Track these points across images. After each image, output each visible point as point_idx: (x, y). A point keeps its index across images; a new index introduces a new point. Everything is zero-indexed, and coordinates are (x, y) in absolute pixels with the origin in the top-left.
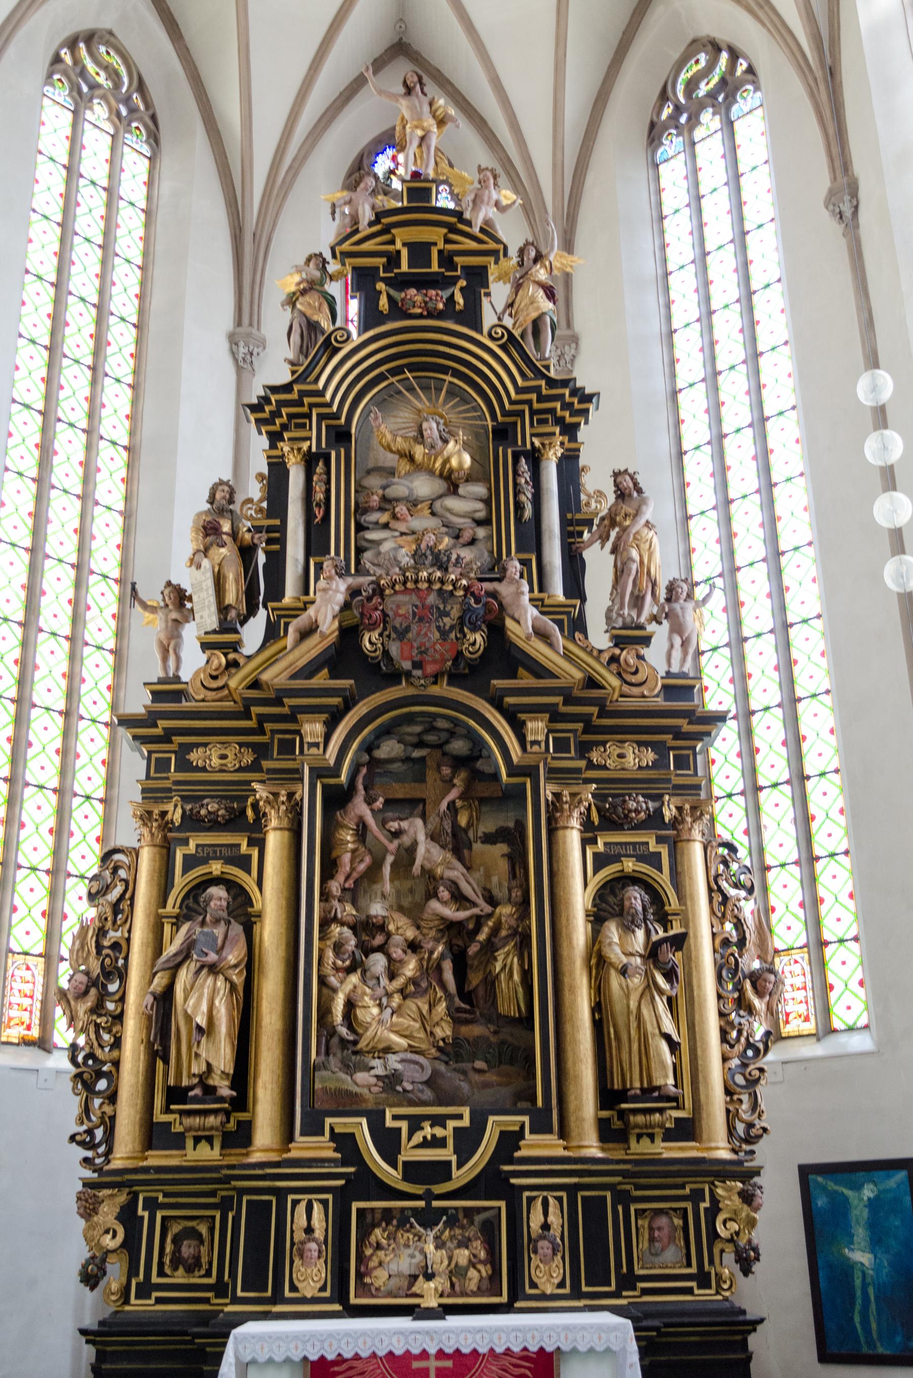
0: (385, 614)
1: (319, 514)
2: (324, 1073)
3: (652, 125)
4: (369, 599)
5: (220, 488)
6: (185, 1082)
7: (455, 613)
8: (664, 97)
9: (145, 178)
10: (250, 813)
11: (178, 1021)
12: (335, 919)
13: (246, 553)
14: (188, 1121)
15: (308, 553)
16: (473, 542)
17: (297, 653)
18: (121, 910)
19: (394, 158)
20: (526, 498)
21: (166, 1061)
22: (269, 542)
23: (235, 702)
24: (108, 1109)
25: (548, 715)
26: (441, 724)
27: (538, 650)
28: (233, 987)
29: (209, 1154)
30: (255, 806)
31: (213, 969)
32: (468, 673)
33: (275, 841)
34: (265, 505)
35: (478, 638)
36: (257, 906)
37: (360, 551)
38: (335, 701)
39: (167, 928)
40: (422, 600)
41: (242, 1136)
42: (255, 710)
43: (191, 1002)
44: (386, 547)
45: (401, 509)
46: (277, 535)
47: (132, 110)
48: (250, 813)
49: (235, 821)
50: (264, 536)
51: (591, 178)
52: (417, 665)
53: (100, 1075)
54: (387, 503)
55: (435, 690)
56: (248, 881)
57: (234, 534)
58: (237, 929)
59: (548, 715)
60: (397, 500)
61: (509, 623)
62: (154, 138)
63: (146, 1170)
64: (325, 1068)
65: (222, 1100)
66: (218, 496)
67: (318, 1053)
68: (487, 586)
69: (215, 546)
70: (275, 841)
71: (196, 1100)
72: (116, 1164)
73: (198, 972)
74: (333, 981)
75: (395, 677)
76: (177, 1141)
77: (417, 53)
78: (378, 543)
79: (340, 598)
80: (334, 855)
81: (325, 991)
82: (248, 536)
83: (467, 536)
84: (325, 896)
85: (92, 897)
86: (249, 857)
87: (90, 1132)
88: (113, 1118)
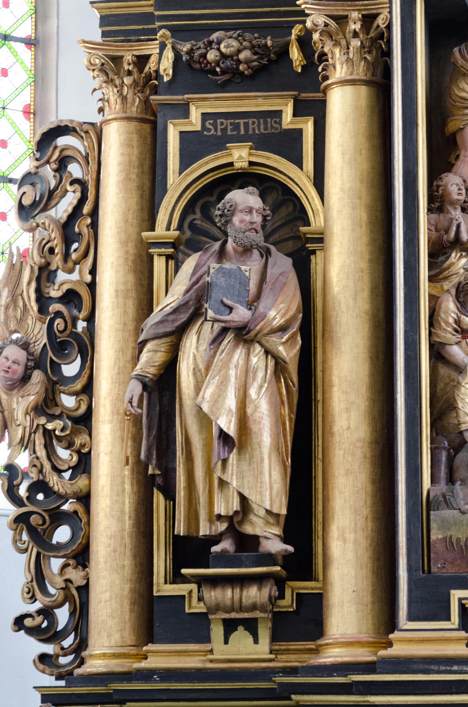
2: (447, 513)
6: (204, 530)
10: (295, 54)
11: (187, 424)
12: (457, 243)
14: (213, 595)
18: (77, 233)
21: (170, 495)
24: (76, 576)
28: (280, 367)
29: (249, 649)
30: (305, 42)
31: (244, 334)
33: (344, 106)
36: (317, 223)
39: (159, 265)
41: (306, 620)
43: (209, 392)
48: (295, 54)
49: (269, 71)
53: (58, 518)
56: (299, 179)
58: (282, 264)
63: (146, 675)
64: (449, 505)
65: (269, 559)
67: (434, 480)
70: (344, 106)
71: (224, 559)
72: (94, 665)
73: (217, 340)
74: (457, 352)
76: (195, 629)
80: (452, 127)
81: (443, 370)
84: (438, 202)
85: (24, 211)
86: (298, 134)
87: (47, 612)
88: (84, 590)
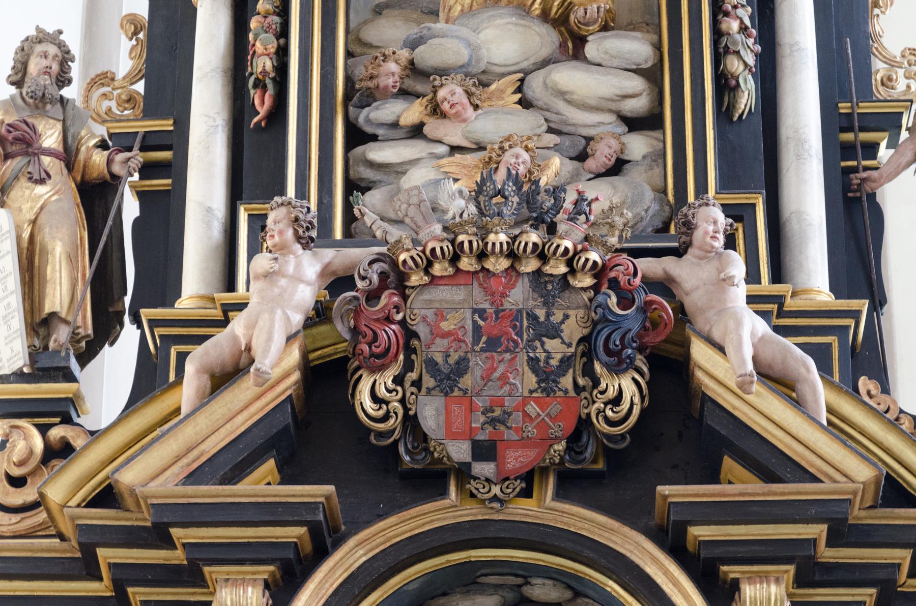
0: (410, 334)
1: (262, 104)
4: (373, 296)
5: (39, 48)
7: (574, 329)
13: (96, 196)
15: (236, 193)
16: (617, 167)
17: (202, 422)
20: (742, 65)
22: (148, 170)
23: (61, 537)
25: (791, 569)
26: (541, 590)
27: (765, 412)
32: (603, 469)
34: (140, 87)
35: (628, 387)
37: (353, 186)
38: (294, 533)
40: (497, 297)
42: (106, 555)
44: (417, 177)
45: (451, 92)
46: (166, 155)
50: (138, 157)
52: (484, 451)
54: (419, 78)
55: (526, 510)
57: (68, 155)
59: (791, 569)
60: (443, 72)
61: (700, 352)
66: (34, 67)
68: (646, 265)
69: (23, 182)
75: (431, 480)
78: (396, 170)
79: (306, 295)
82: (99, 158)
83: (603, 155)
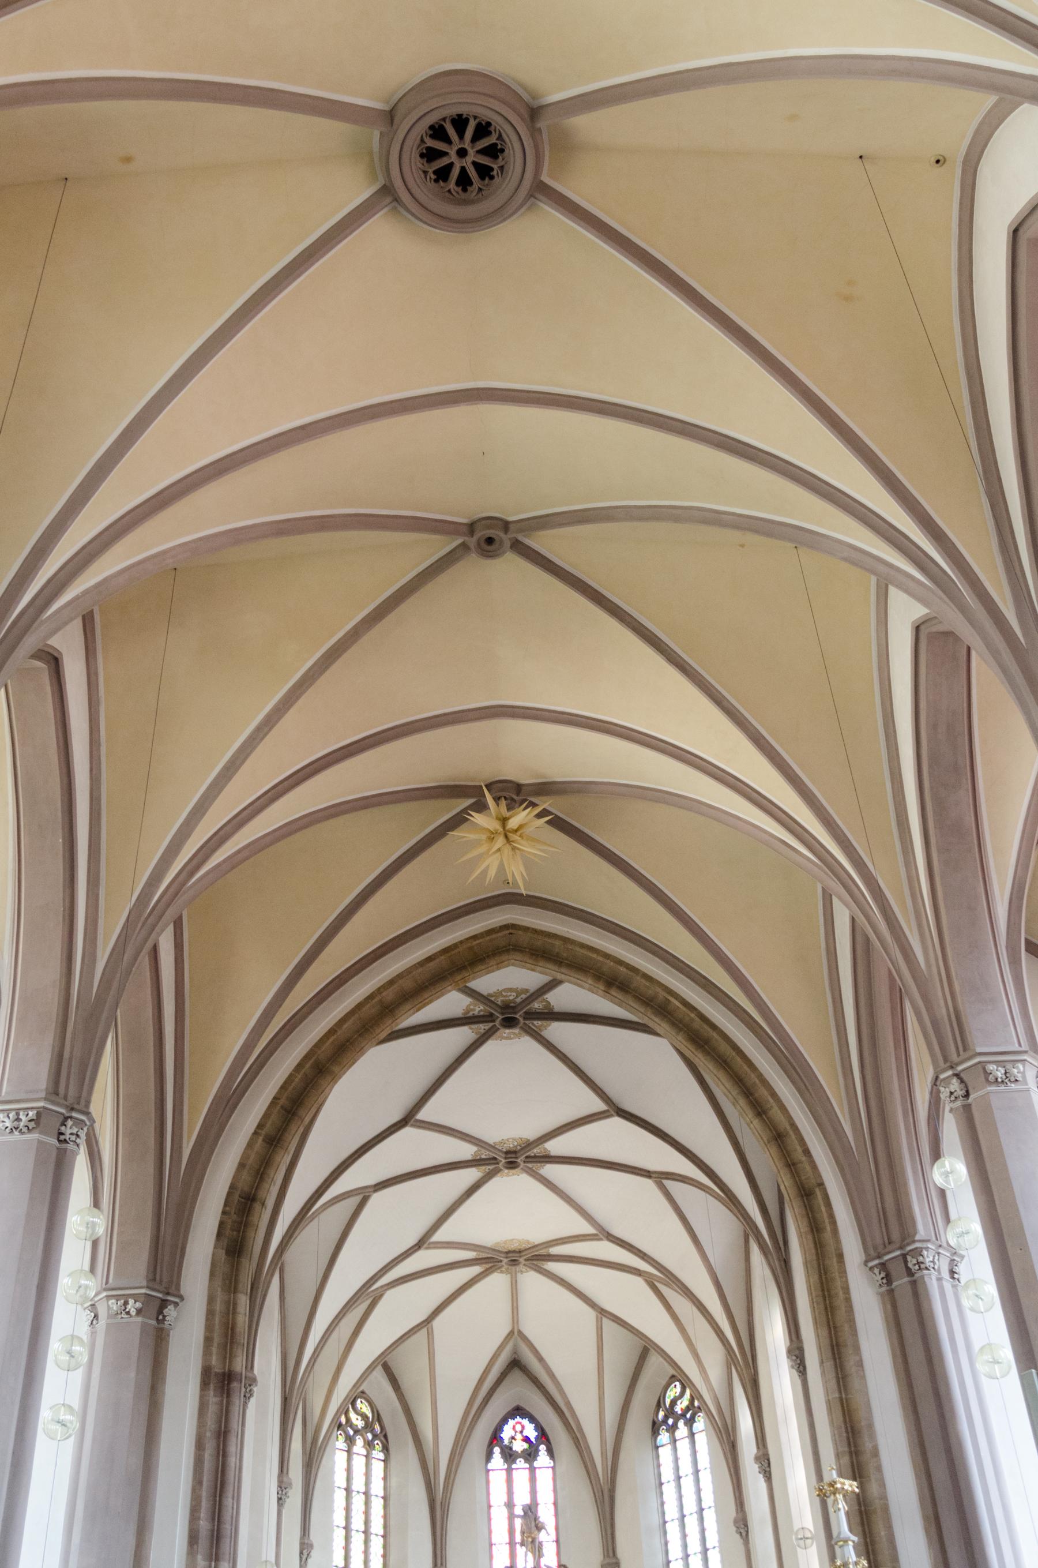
3: (654, 1423)
8: (659, 1406)
9: (382, 1475)
19: (514, 1427)
47: (375, 1436)
51: (623, 1456)
62: (386, 1449)
77: (525, 1366)
